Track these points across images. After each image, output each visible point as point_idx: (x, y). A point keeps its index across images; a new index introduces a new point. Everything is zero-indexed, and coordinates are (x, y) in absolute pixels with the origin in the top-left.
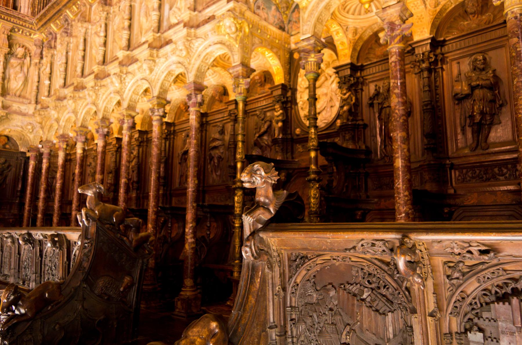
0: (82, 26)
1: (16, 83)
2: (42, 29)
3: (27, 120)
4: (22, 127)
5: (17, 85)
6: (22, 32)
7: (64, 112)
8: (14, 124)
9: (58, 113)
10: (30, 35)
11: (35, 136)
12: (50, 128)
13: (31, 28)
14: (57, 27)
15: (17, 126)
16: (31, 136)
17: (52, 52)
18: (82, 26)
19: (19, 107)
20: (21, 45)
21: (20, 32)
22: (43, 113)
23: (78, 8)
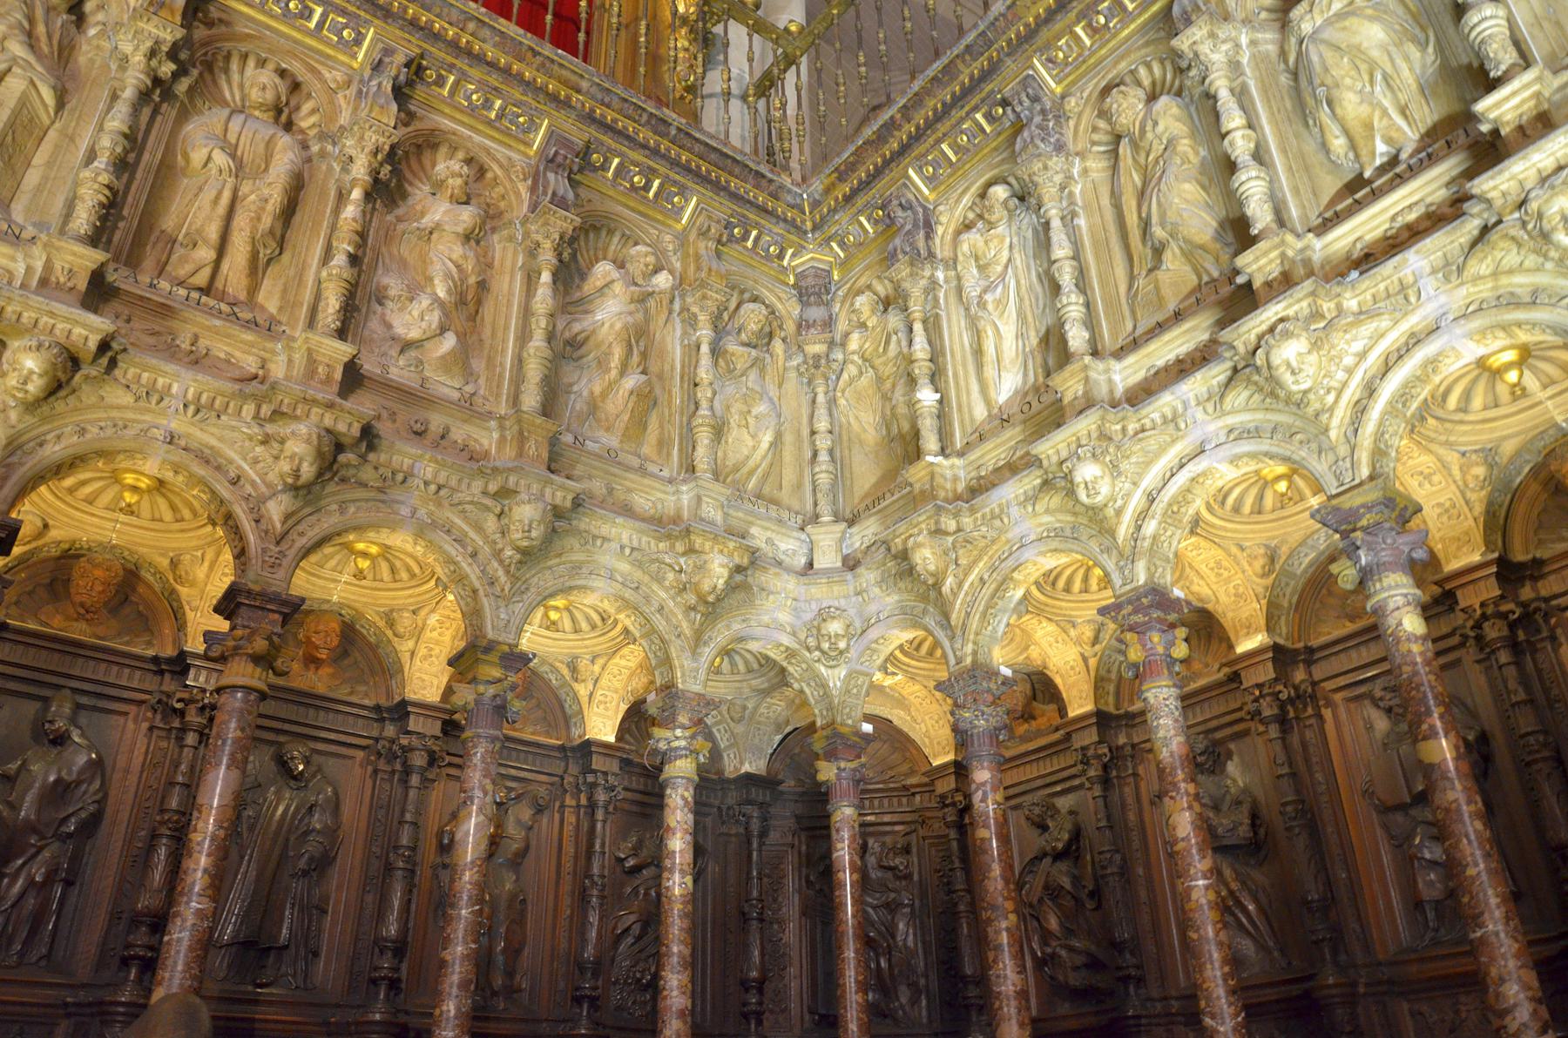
0: (1212, 35)
1: (750, 443)
2: (843, 217)
3: (820, 593)
4: (794, 634)
5: (754, 448)
6: (757, 239)
7: (1148, 464)
8: (766, 619)
9: (1114, 470)
10: (781, 256)
11: (849, 676)
12: (997, 590)
13: (793, 225)
14: (929, 180)
15: (780, 628)
16: (835, 677)
17: (927, 273)
18: (1212, 35)
19: (769, 541)
20: (747, 296)
21: (749, 244)
22: (951, 525)
23: (1093, 30)
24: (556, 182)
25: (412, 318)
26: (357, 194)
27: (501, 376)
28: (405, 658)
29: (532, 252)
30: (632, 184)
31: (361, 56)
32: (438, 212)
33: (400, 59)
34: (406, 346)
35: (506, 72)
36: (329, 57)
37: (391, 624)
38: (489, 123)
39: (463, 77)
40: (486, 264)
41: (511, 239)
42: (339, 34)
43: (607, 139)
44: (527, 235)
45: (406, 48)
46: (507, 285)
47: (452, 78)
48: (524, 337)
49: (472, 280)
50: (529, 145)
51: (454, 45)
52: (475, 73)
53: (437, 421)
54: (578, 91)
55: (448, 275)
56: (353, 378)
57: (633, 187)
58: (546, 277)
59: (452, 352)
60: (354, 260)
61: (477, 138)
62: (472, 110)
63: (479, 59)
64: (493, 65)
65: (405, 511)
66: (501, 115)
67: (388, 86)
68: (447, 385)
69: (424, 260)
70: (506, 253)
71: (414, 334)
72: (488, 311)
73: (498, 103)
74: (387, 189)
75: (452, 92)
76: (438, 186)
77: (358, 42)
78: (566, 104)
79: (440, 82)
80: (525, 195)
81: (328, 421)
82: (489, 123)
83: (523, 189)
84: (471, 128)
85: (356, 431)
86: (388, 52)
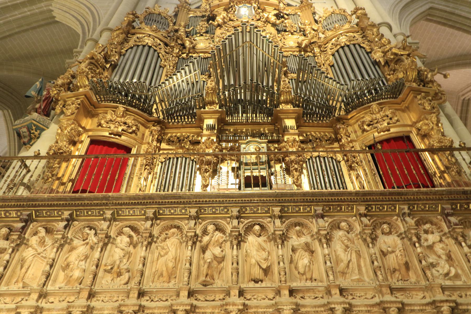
27: (467, 273)
30: (465, 208)
31: (397, 211)
36: (391, 214)
38: (427, 211)
39: (418, 204)
41: (448, 237)
42: (391, 209)
43: (455, 201)
47: (416, 206)
50: (438, 211)
52: (420, 202)
54: (443, 195)
57: (466, 209)
61: (427, 215)
62: (423, 210)
66: (429, 208)
73: (427, 206)
75: (417, 208)
77: (395, 208)
78: (442, 199)
82: (427, 211)
84: (424, 214)
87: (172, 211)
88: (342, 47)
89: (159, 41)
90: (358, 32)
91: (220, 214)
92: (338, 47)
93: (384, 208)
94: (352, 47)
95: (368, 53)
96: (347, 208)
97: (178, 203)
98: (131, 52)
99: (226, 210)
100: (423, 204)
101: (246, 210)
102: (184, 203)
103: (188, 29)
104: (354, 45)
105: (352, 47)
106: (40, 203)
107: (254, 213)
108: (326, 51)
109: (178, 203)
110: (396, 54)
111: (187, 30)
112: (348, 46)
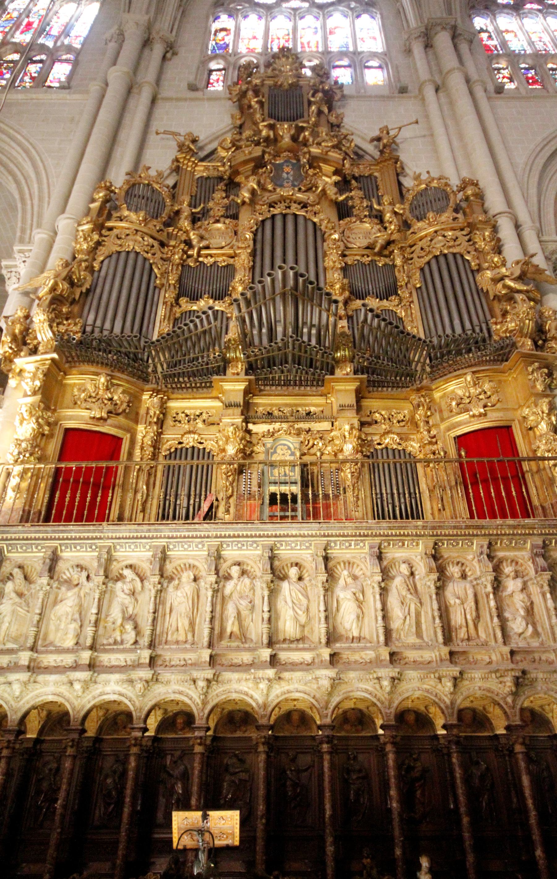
24: (541, 561)
25: (517, 625)
26: (491, 596)
28: (551, 719)
29: (542, 587)
32: (512, 585)
33: (485, 547)
34: (520, 635)
35: (513, 534)
37: (544, 710)
40: (529, 596)
41: (533, 584)
43: (549, 537)
44: (538, 582)
45: (485, 543)
46: (538, 599)
48: (549, 618)
49: (528, 604)
50: (526, 548)
51: (497, 535)
52: (505, 537)
53: (537, 656)
55: (523, 607)
56: (512, 653)
58: (548, 596)
59: (533, 632)
60: (498, 616)
63: (505, 534)
64: (509, 535)
65: (539, 688)
67: (486, 557)
68: (535, 643)
69: (513, 602)
70: (534, 589)
71: (521, 631)
72: (536, 610)
74: (497, 585)
76: (508, 576)
77: (472, 544)
78: (533, 534)
79: (496, 543)
80: (532, 565)
81: (513, 674)
83: (530, 563)
85: (520, 674)
86: (482, 547)
87: (186, 546)
88: (436, 257)
89: (151, 240)
90: (462, 230)
91: (247, 549)
92: (430, 256)
93: (458, 544)
94: (451, 258)
95: (472, 271)
96: (412, 544)
97: (193, 537)
98: (110, 262)
99: (255, 545)
100: (507, 540)
101: (282, 545)
102: (201, 537)
103: (195, 207)
104: (454, 255)
105: (451, 258)
106: (13, 536)
107: (292, 549)
108: (412, 259)
109: (193, 537)
110: (509, 287)
111: (194, 210)
112: (445, 255)
